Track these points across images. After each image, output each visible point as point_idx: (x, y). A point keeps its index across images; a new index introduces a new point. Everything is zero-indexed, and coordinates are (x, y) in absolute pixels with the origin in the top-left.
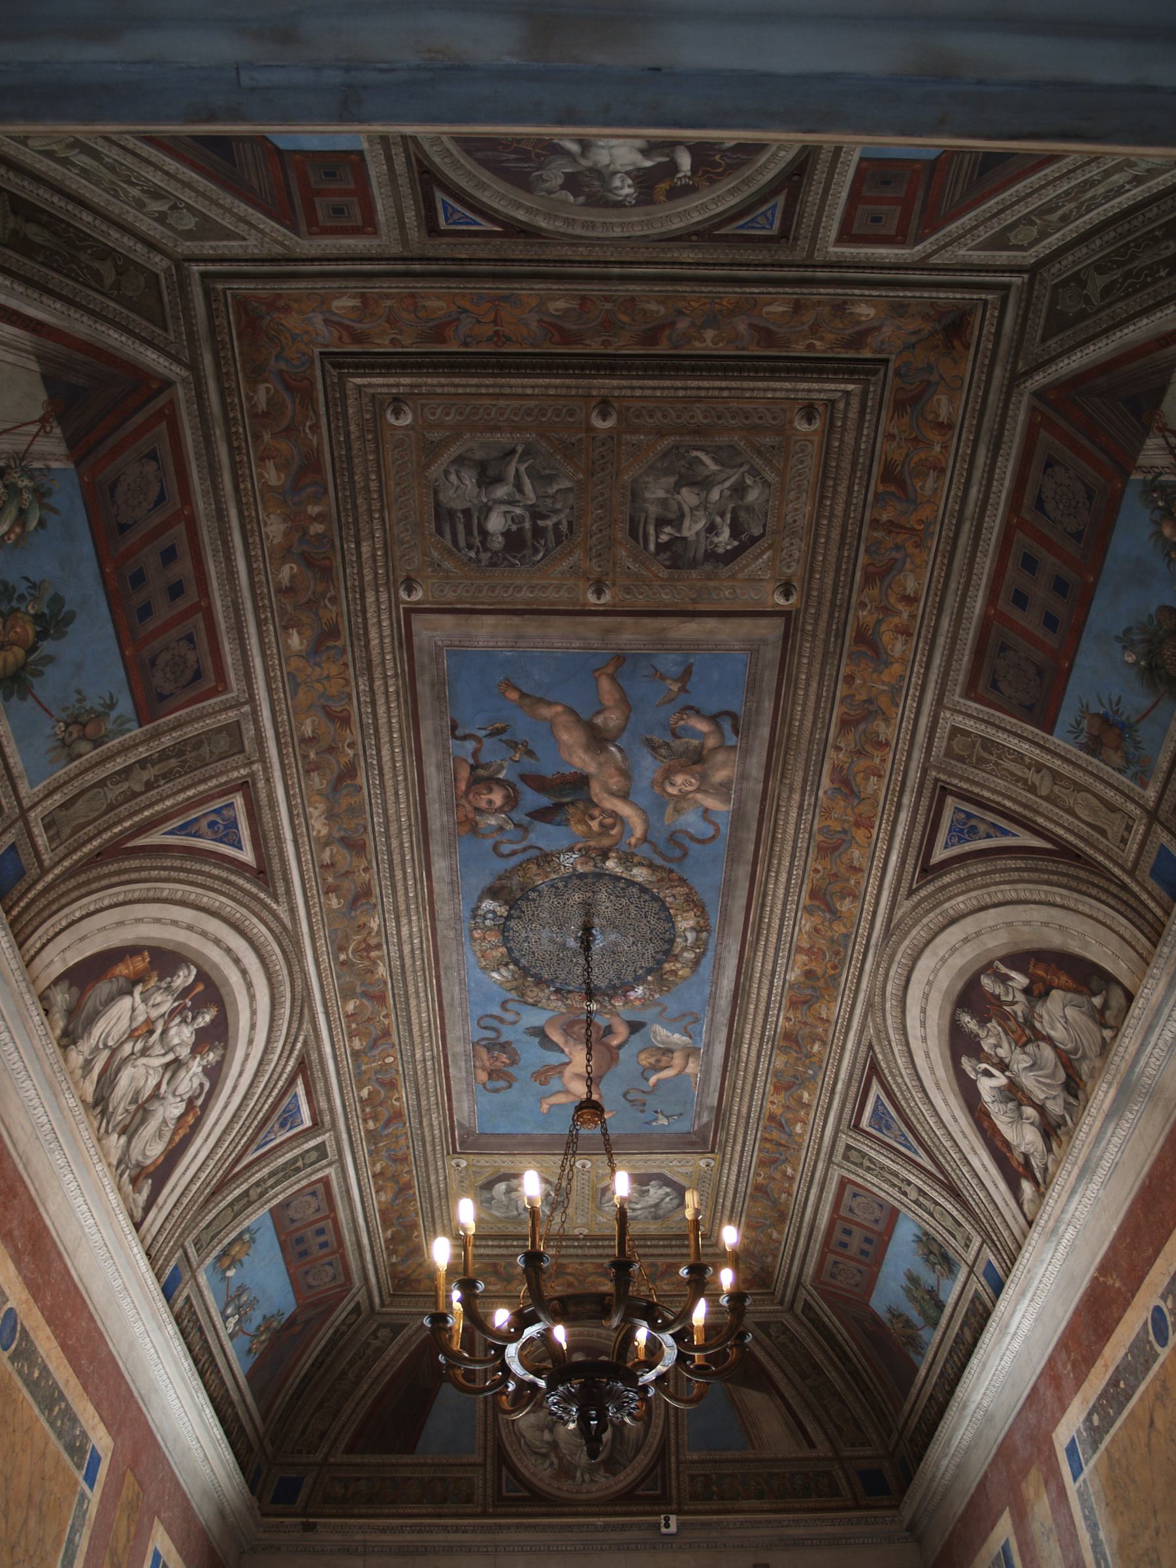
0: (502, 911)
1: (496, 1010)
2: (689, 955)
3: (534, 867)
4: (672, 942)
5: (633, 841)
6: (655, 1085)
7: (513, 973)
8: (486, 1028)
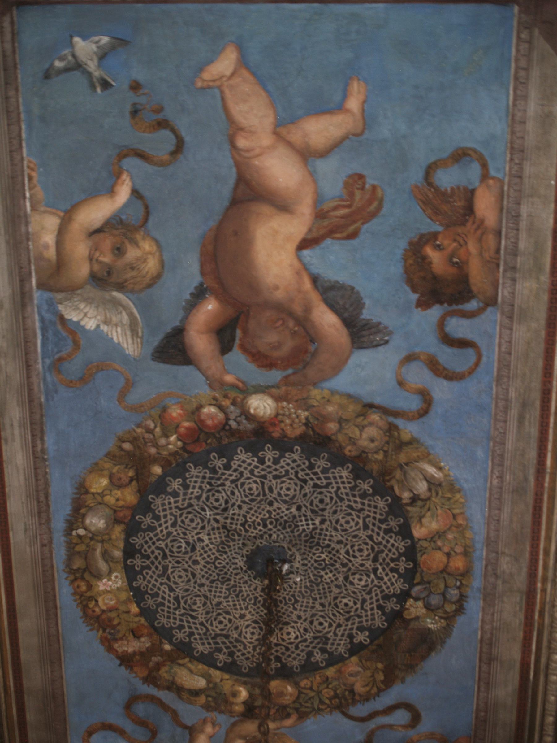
0: (415, 608)
1: (441, 390)
2: (96, 522)
3: (359, 688)
4: (130, 552)
5: (209, 729)
6: (118, 175)
7: (404, 484)
8: (463, 344)
